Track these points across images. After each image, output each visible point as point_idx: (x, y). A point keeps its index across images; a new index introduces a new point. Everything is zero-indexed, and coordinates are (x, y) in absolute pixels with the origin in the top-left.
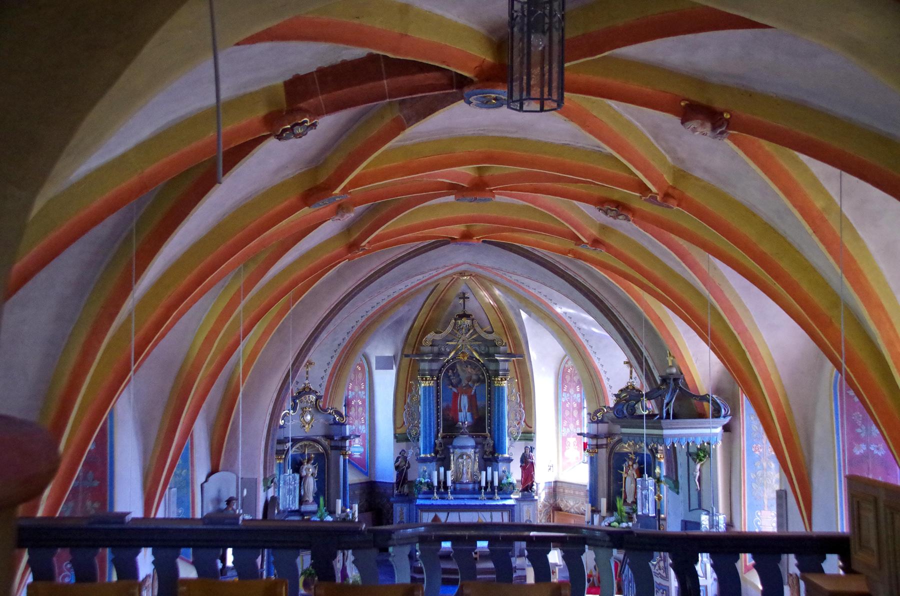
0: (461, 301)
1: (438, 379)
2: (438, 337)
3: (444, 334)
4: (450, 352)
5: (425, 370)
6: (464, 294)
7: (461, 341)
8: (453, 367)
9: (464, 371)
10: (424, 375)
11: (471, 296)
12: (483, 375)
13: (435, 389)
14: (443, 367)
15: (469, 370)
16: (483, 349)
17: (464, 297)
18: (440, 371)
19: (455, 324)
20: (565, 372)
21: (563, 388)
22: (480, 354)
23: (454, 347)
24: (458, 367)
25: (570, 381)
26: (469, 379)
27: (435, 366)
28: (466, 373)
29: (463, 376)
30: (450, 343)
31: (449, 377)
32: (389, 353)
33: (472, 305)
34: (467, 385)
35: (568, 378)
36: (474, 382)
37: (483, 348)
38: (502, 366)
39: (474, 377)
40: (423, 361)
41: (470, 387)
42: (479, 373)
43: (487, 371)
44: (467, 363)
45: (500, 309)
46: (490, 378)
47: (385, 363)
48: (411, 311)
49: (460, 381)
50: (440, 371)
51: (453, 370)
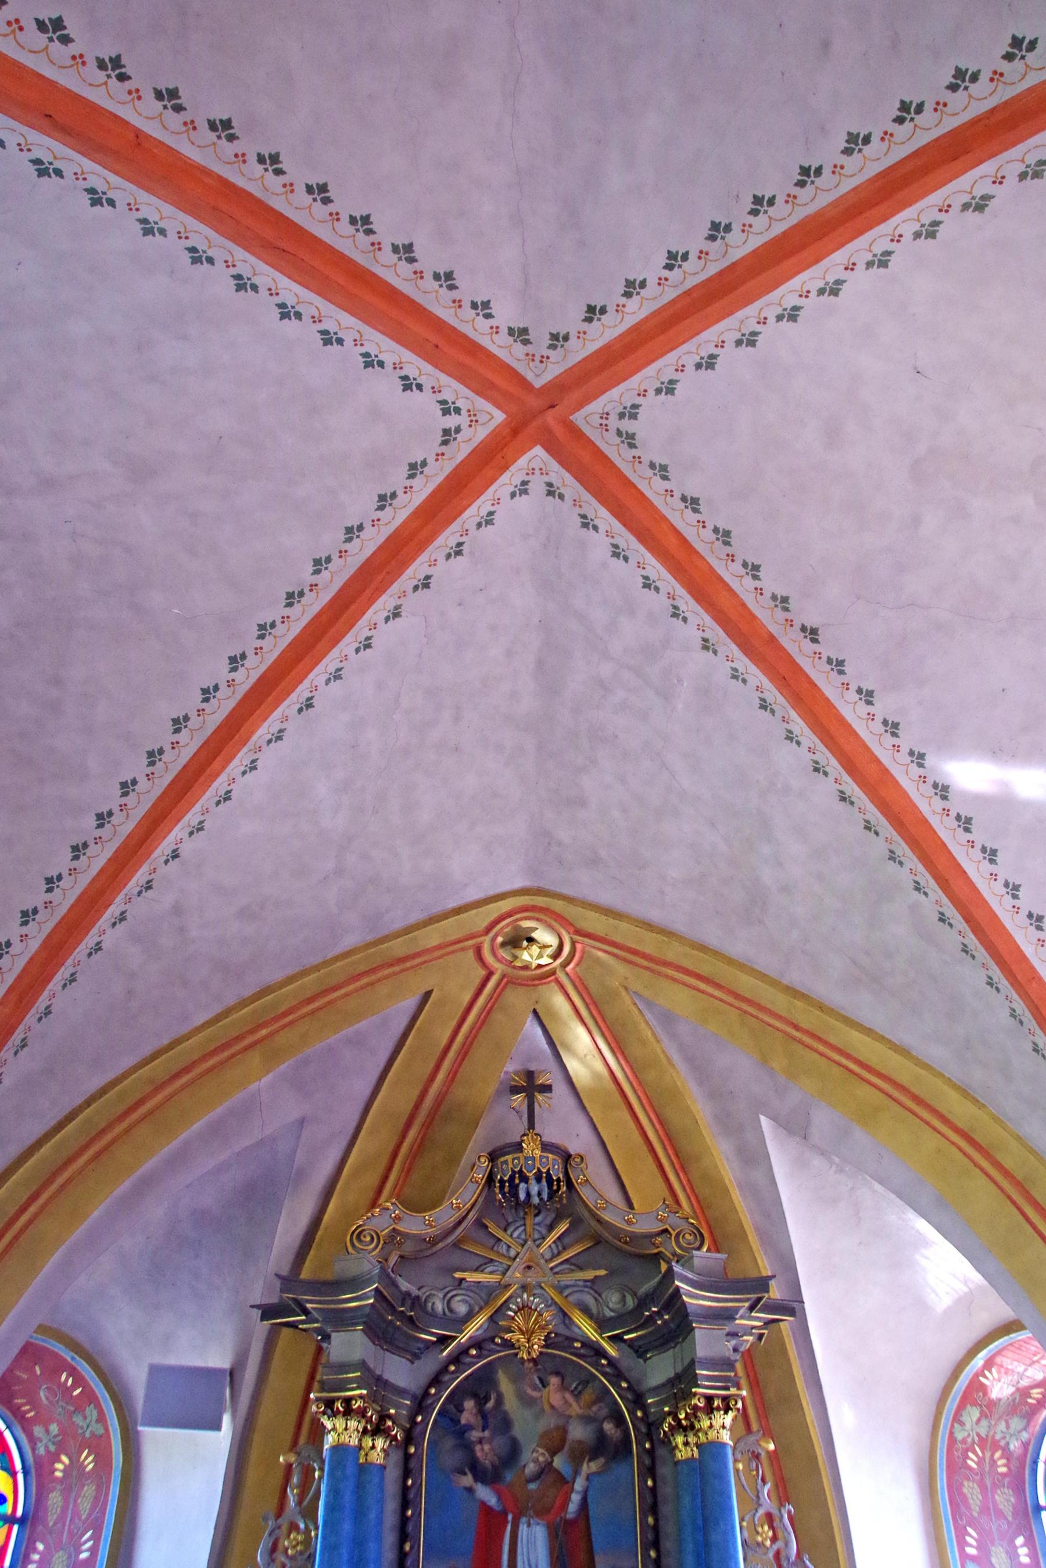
0: (519, 1099)
1: (409, 1439)
2: (414, 1225)
3: (443, 1216)
4: (470, 1316)
5: (344, 1367)
6: (530, 1075)
7: (516, 1274)
8: (481, 1388)
9: (527, 1401)
10: (342, 1386)
11: (560, 1089)
12: (618, 1419)
13: (393, 1474)
14: (436, 1380)
15: (553, 1394)
16: (613, 1301)
17: (530, 1086)
18: (421, 1404)
19: (490, 1180)
20: (956, 1467)
21: (962, 1544)
22: (602, 1324)
23: (490, 1292)
24: (505, 1385)
25: (985, 1510)
26: (555, 1442)
27: (401, 1373)
28: (537, 1414)
29: (528, 1427)
30: (471, 1277)
31: (461, 1432)
32: (218, 1358)
33: (561, 1124)
34: (546, 1469)
35: (971, 1490)
36: (577, 1458)
37: (613, 1299)
38: (706, 1342)
39: (578, 1432)
40: (341, 1319)
41: (564, 1483)
42: (601, 1410)
43: (637, 1400)
44: (545, 1366)
45: (675, 1151)
46: (650, 1427)
47: (190, 1400)
48: (310, 1111)
49: (513, 1454)
50: (421, 1404)
51: (481, 1401)
